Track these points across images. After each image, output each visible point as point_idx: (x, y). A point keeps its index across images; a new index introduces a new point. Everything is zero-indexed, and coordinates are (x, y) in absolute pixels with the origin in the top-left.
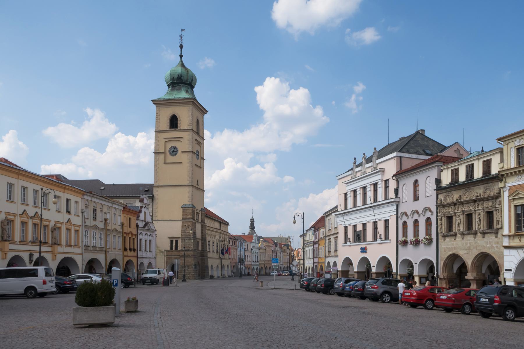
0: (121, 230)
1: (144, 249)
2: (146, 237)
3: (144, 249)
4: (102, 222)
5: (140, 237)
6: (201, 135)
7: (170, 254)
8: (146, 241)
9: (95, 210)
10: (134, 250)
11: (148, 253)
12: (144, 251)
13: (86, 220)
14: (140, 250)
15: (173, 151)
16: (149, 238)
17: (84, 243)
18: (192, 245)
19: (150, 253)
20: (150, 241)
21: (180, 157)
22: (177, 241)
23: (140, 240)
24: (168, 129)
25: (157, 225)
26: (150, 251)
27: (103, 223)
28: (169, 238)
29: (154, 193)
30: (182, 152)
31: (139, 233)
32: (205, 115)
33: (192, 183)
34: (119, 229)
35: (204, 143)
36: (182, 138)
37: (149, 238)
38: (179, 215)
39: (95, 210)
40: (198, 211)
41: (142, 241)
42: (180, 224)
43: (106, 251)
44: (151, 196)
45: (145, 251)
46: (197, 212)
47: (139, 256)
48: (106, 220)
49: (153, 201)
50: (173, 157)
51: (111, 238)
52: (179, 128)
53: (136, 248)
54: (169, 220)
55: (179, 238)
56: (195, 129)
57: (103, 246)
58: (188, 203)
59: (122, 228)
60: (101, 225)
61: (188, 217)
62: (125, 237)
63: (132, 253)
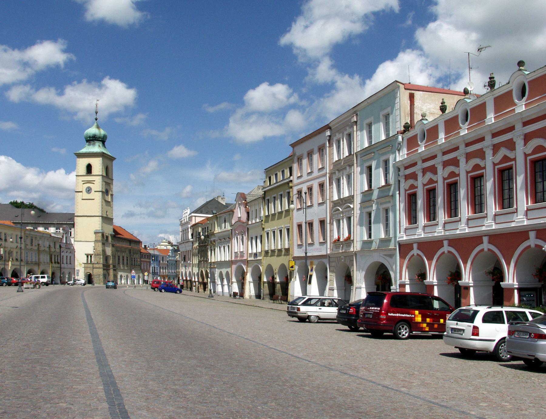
0: (49, 251)
1: (65, 262)
2: (67, 254)
3: (65, 262)
4: (36, 246)
5: (62, 254)
6: (110, 177)
7: (86, 265)
8: (67, 257)
9: (32, 240)
10: (58, 263)
11: (69, 265)
12: (65, 263)
13: (27, 246)
14: (63, 263)
15: (89, 191)
16: (69, 255)
17: (26, 260)
18: (102, 260)
19: (70, 265)
20: (70, 257)
21: (93, 195)
22: (91, 257)
23: (63, 256)
24: (85, 174)
25: (77, 246)
26: (70, 264)
27: (37, 246)
28: (86, 254)
29: (75, 221)
30: (95, 191)
31: (61, 252)
32: (114, 161)
33: (102, 214)
34: (47, 249)
35: (113, 182)
36: (94, 181)
37: (69, 255)
38: (93, 237)
39: (32, 240)
40: (107, 235)
41: (64, 257)
42: (92, 244)
43: (39, 264)
44: (72, 223)
45: (67, 263)
46: (106, 236)
47: (62, 267)
48: (39, 245)
49: (74, 227)
50: (88, 195)
51: (42, 257)
52: (92, 174)
53: (59, 261)
54: (85, 240)
55: (93, 254)
56: (105, 175)
57: (37, 261)
58: (99, 229)
59: (50, 249)
60: (36, 248)
61: (99, 239)
62: (51, 255)
63: (57, 265)
